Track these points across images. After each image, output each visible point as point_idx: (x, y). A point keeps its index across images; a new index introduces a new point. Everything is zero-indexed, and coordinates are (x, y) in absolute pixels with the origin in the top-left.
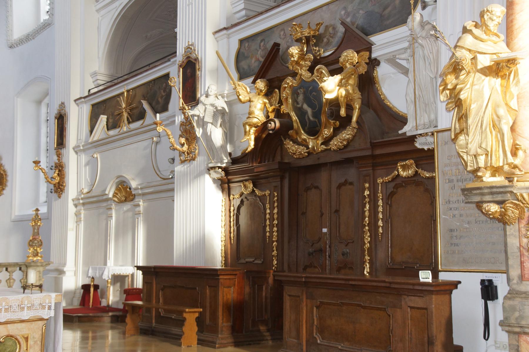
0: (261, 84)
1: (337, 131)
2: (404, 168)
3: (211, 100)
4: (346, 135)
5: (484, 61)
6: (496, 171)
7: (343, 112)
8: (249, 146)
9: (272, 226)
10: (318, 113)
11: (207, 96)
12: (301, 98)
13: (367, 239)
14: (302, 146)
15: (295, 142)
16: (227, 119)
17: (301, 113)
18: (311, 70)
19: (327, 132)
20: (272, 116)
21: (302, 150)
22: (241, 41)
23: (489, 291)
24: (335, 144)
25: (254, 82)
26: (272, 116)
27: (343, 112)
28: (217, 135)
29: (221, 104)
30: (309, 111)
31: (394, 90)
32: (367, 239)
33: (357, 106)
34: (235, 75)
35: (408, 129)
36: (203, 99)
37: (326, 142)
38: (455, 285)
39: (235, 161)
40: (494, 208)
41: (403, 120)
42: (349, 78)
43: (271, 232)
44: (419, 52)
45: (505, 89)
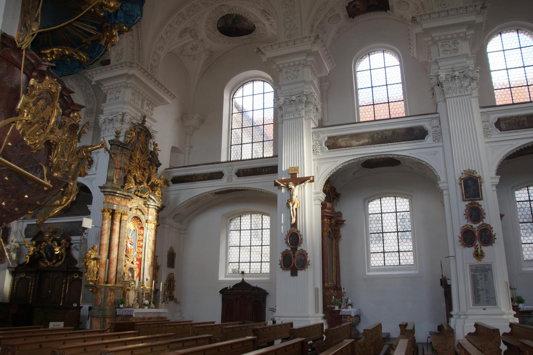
0: (34, 243)
1: (57, 262)
2: (76, 275)
3: (14, 243)
4: (60, 263)
5: (93, 256)
6: (92, 281)
7: (60, 258)
8: (26, 261)
9: (31, 289)
10: (52, 256)
11: (12, 242)
12: (47, 250)
13: (62, 295)
14: (46, 264)
15: (43, 262)
16: (19, 251)
17: (46, 253)
18: (52, 242)
19: (54, 261)
20: (36, 253)
21: (45, 265)
22: (28, 225)
23: (90, 308)
24: (56, 265)
25: (32, 240)
26: (36, 253)
27: (60, 258)
28: (14, 256)
29: (17, 245)
30: (50, 254)
31: (76, 254)
32: (62, 295)
33: (64, 256)
34: (24, 236)
35: (77, 266)
36: (10, 242)
37: (54, 264)
38: (82, 307)
39: (19, 265)
40: (91, 290)
41: (76, 262)
42: (62, 248)
43: (31, 291)
44: (82, 247)
45: (97, 262)
